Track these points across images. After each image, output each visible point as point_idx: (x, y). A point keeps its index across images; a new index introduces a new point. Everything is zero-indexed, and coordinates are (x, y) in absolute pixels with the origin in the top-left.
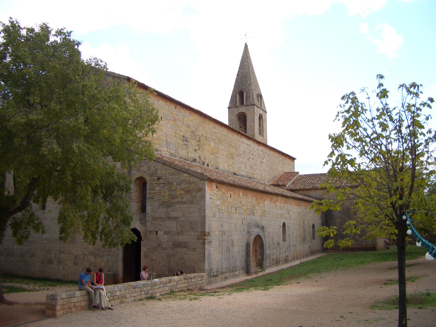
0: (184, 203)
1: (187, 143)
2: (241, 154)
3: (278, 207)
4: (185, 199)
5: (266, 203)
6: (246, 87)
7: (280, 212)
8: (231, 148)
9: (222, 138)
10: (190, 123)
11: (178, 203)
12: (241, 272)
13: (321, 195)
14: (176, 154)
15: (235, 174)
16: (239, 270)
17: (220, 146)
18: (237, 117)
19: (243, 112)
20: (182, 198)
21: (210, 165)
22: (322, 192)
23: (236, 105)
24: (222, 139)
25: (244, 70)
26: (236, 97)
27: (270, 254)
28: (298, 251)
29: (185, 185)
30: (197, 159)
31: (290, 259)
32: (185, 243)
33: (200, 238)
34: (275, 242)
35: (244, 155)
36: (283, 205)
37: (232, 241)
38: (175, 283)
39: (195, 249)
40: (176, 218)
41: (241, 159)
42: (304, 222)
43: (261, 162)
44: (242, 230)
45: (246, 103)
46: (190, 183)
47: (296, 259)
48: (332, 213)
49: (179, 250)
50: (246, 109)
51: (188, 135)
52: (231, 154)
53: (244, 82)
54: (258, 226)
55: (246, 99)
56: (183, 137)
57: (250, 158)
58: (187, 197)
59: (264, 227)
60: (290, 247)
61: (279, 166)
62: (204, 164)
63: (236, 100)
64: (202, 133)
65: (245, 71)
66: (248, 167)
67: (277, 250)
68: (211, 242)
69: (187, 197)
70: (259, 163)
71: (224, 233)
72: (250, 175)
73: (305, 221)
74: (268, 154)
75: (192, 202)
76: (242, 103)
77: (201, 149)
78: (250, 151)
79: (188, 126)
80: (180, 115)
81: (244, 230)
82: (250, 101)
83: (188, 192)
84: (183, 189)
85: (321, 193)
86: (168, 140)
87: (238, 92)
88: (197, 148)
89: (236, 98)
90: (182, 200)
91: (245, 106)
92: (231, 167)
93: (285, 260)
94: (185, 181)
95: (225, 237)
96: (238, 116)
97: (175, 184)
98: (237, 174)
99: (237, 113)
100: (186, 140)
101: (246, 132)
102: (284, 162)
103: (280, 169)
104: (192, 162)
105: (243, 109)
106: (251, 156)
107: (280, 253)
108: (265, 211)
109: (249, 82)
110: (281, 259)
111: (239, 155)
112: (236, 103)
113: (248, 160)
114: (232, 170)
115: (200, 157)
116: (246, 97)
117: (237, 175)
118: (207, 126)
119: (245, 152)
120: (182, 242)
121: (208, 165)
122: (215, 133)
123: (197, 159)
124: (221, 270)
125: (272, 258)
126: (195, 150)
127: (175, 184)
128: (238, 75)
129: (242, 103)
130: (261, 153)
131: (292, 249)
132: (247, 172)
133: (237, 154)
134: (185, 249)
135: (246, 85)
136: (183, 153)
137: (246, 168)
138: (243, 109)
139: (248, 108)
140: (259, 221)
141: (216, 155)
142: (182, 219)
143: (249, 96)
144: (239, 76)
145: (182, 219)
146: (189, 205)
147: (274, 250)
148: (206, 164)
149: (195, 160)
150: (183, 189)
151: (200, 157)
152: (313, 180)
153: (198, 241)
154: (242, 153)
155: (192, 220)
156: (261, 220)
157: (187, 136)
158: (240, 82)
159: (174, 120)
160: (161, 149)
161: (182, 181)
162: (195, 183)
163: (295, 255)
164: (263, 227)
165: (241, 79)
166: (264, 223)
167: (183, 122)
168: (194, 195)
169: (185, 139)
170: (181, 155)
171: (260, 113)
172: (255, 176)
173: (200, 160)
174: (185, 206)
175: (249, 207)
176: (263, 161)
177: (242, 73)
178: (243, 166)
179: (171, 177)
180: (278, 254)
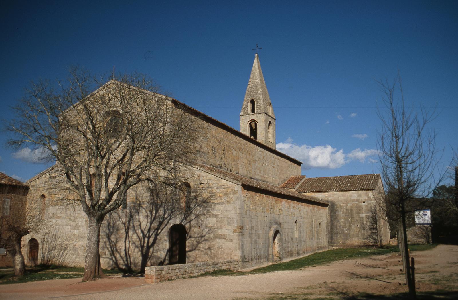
0: (223, 203)
1: (215, 152)
2: (256, 160)
3: (291, 208)
4: (223, 200)
5: (282, 204)
6: (257, 96)
7: (293, 211)
8: (248, 155)
9: (242, 147)
11: (218, 204)
12: (265, 260)
13: (327, 197)
15: (252, 178)
16: (264, 258)
17: (240, 153)
20: (221, 199)
21: (232, 171)
22: (328, 195)
23: (248, 113)
24: (241, 148)
26: (248, 105)
27: (286, 247)
28: (307, 246)
29: (223, 189)
30: (223, 165)
31: (301, 252)
32: (224, 235)
33: (236, 231)
34: (290, 237)
35: (259, 162)
36: (295, 206)
37: (258, 234)
38: (221, 265)
39: (231, 240)
40: (216, 215)
41: (256, 165)
42: (312, 221)
43: (273, 167)
44: (265, 226)
45: (257, 111)
46: (228, 187)
47: (306, 253)
48: (337, 214)
49: (218, 241)
50: (257, 117)
52: (248, 160)
53: (255, 91)
54: (276, 223)
55: (257, 107)
56: (212, 147)
57: (264, 163)
58: (225, 198)
59: (282, 224)
60: (301, 242)
61: (287, 171)
62: (228, 170)
63: (248, 109)
66: (262, 172)
67: (291, 244)
68: (244, 234)
69: (225, 198)
70: (271, 168)
71: (252, 228)
72: (264, 179)
73: (313, 220)
74: (279, 159)
75: (229, 203)
76: (253, 111)
78: (264, 157)
81: (267, 226)
82: (261, 109)
83: (226, 194)
84: (222, 192)
85: (327, 196)
88: (223, 156)
89: (248, 107)
90: (221, 201)
91: (256, 114)
92: (248, 172)
93: (297, 253)
94: (223, 186)
95: (254, 231)
97: (215, 188)
99: (249, 120)
100: (215, 150)
101: (256, 137)
102: (292, 166)
103: (289, 173)
105: (254, 117)
106: (265, 162)
107: (293, 247)
108: (282, 210)
110: (294, 252)
111: (255, 162)
112: (248, 111)
113: (262, 165)
114: (250, 175)
115: (225, 164)
116: (257, 105)
117: (253, 179)
118: (230, 137)
119: (260, 158)
120: (221, 235)
121: (231, 171)
122: (236, 142)
124: (251, 257)
125: (287, 251)
127: (215, 188)
129: (253, 111)
130: (272, 159)
131: (303, 244)
132: (262, 176)
133: (253, 160)
134: (223, 241)
135: (256, 94)
137: (260, 173)
138: (254, 117)
139: (259, 116)
140: (278, 219)
141: (237, 162)
142: (220, 216)
143: (260, 105)
145: (220, 216)
146: (227, 205)
147: (289, 244)
148: (229, 170)
150: (222, 192)
151: (225, 164)
152: (319, 184)
153: (234, 233)
155: (229, 216)
156: (279, 218)
157: (215, 146)
158: (251, 91)
161: (221, 186)
162: (232, 187)
163: (306, 250)
164: (280, 224)
166: (281, 221)
168: (230, 197)
171: (270, 120)
172: (268, 180)
173: (225, 166)
174: (224, 205)
175: (270, 207)
176: (274, 166)
177: (253, 83)
178: (258, 171)
179: (212, 182)
180: (292, 247)
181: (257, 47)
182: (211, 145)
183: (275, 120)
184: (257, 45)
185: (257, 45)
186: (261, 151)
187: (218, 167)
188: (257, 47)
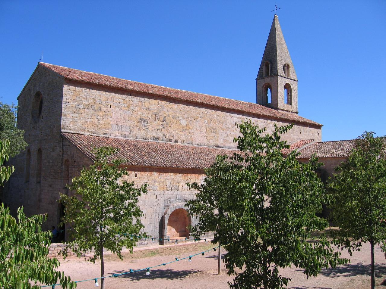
8: (212, 123)
10: (151, 106)
14: (131, 135)
15: (218, 147)
18: (264, 88)
19: (269, 83)
25: (272, 41)
41: (228, 132)
51: (147, 117)
53: (271, 53)
55: (271, 70)
56: (141, 119)
62: (170, 140)
64: (167, 113)
65: (272, 42)
77: (166, 128)
79: (148, 109)
80: (137, 100)
86: (120, 124)
87: (265, 64)
91: (270, 77)
92: (211, 141)
96: (265, 86)
98: (221, 146)
100: (145, 122)
104: (153, 140)
105: (268, 80)
109: (275, 53)
112: (263, 74)
117: (222, 147)
121: (176, 141)
123: (160, 137)
126: (158, 130)
128: (266, 47)
136: (141, 133)
144: (267, 48)
148: (173, 141)
149: (158, 138)
154: (230, 126)
158: (268, 54)
159: (129, 106)
160: (110, 132)
165: (268, 51)
167: (140, 107)
169: (143, 121)
170: (136, 136)
177: (269, 46)
181: (276, 7)
182: (139, 117)
183: (297, 81)
184: (276, 5)
185: (276, 5)
186: (237, 118)
187: (152, 138)
188: (276, 7)
